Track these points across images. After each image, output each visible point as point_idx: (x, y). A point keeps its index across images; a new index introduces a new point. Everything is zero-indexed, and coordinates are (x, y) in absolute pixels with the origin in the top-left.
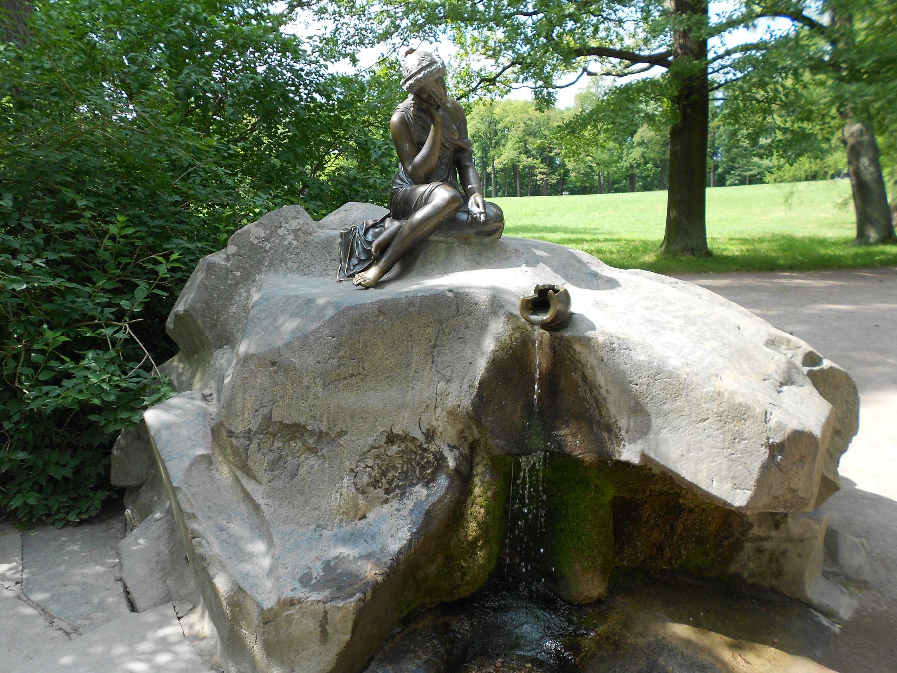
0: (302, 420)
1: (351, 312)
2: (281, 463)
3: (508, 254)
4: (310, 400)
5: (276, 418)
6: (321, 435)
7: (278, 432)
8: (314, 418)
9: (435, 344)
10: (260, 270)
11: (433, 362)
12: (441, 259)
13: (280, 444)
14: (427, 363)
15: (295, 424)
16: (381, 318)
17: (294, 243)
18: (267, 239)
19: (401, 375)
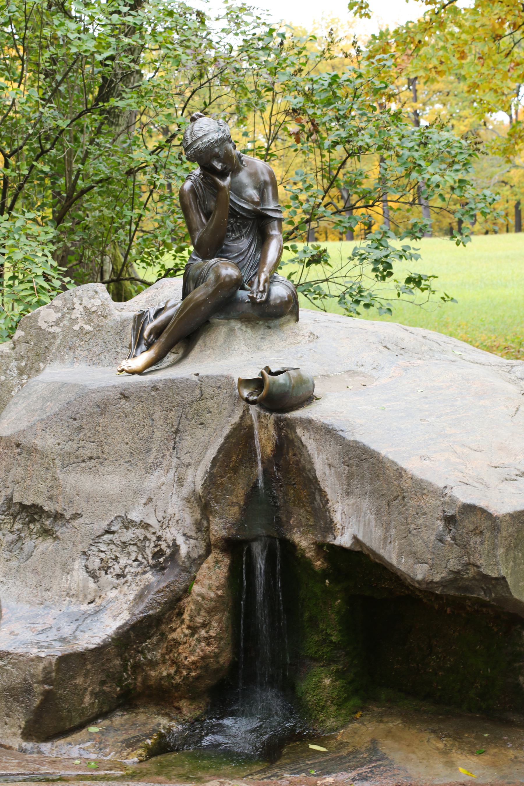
0: (39, 501)
1: (93, 395)
2: (19, 544)
3: (300, 338)
4: (48, 481)
5: (16, 499)
6: (58, 517)
7: (18, 514)
8: (50, 498)
10: (45, 358)
11: (174, 448)
12: (219, 344)
13: (20, 526)
14: (168, 450)
15: (33, 505)
16: (124, 401)
17: (87, 328)
18: (57, 323)
19: (140, 460)
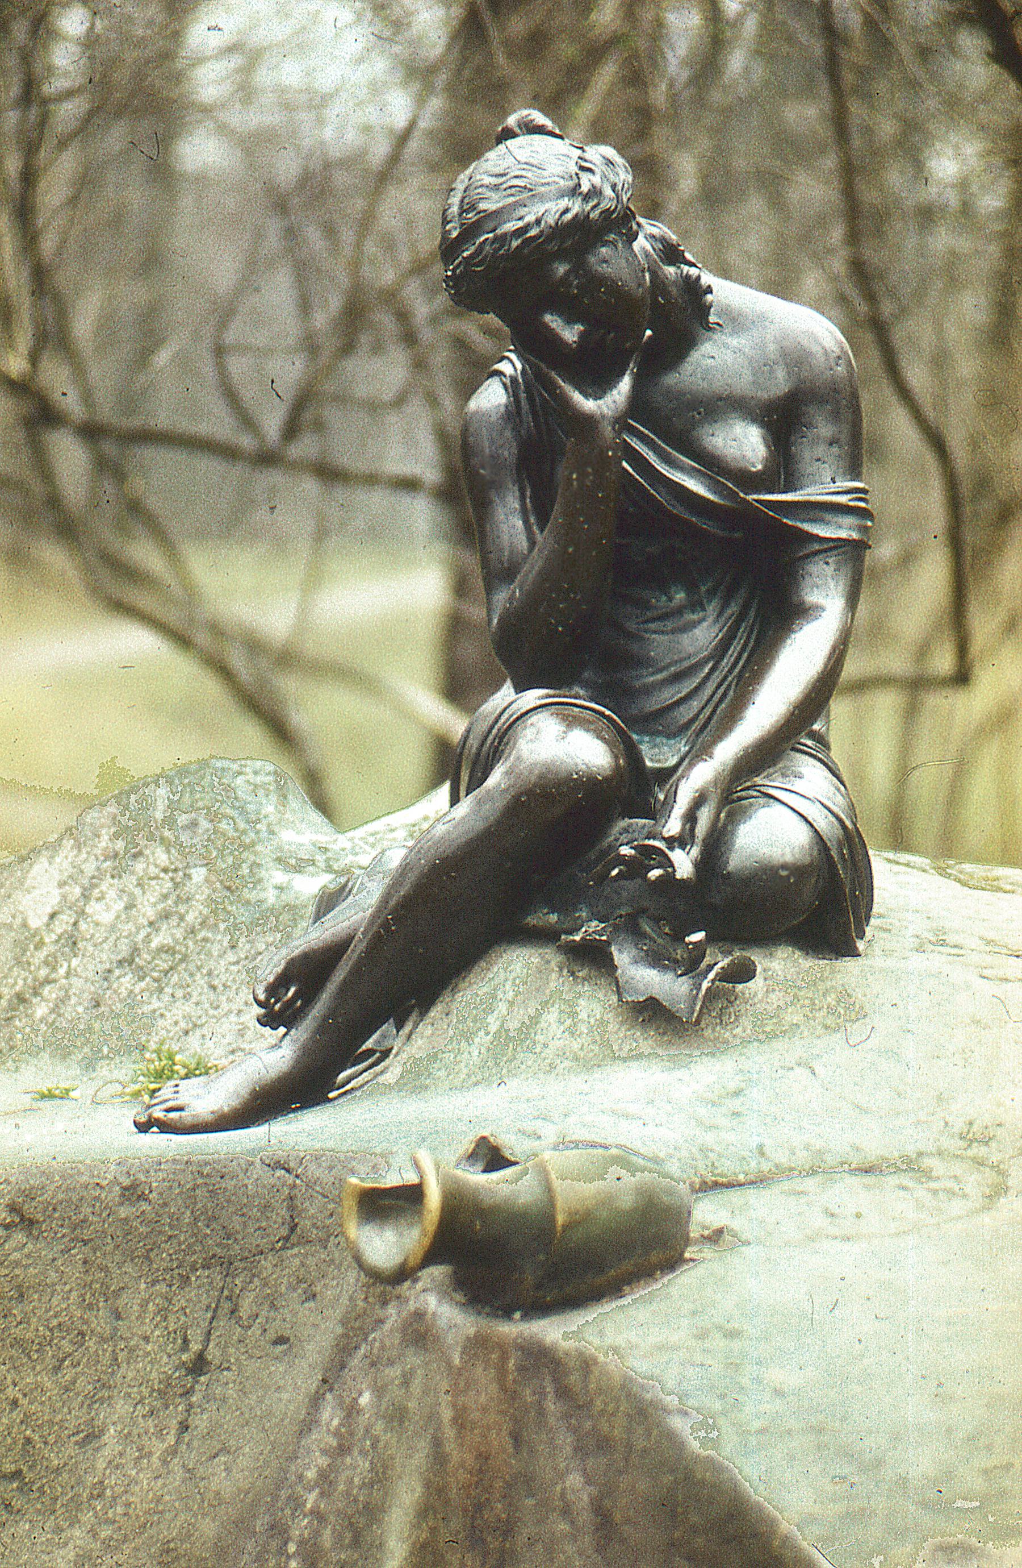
9: (201, 1357)
16: (19, 1237)
